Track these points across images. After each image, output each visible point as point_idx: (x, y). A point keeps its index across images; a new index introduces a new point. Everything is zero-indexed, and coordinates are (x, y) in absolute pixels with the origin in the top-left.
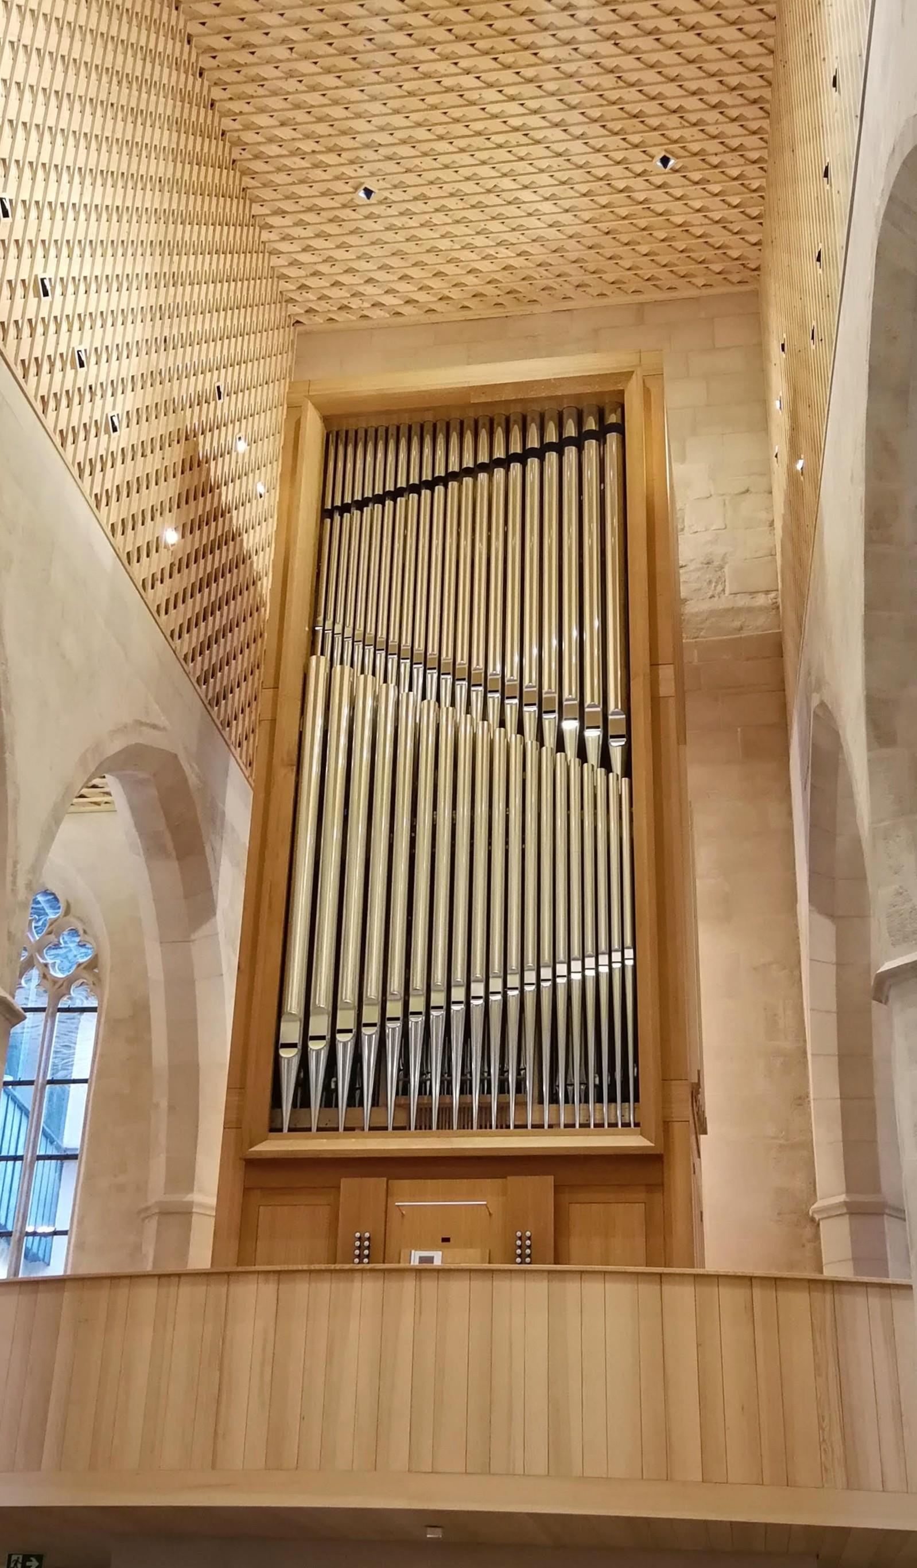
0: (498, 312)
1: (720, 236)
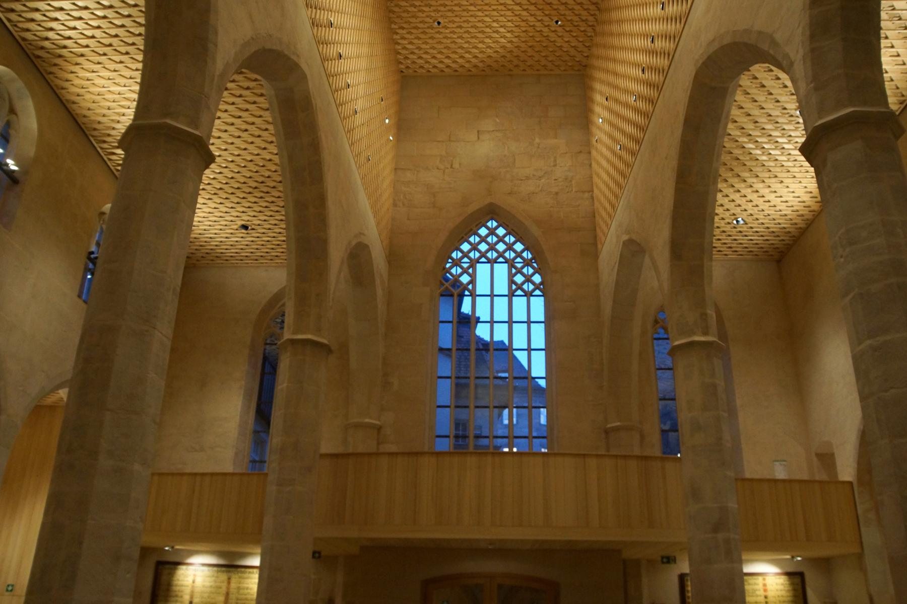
0: (483, 73)
1: (573, 52)
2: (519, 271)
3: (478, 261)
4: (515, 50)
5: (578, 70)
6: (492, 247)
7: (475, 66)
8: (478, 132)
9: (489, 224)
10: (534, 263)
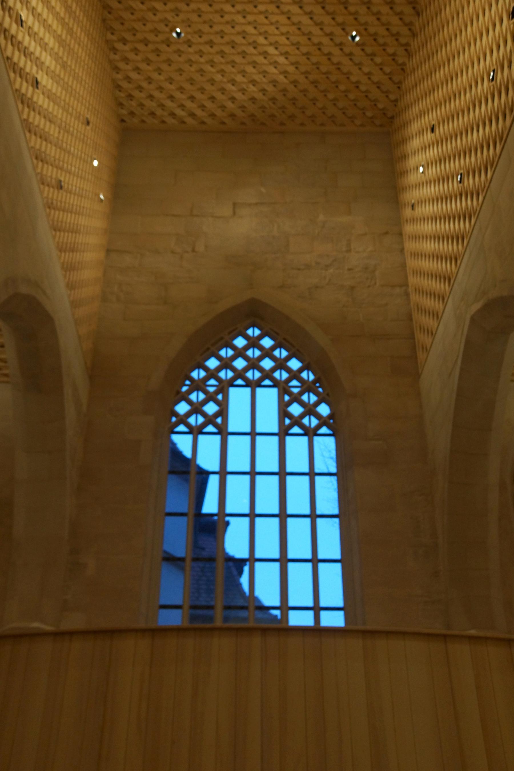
2: (296, 399)
3: (231, 383)
4: (291, 88)
5: (381, 126)
6: (253, 364)
7: (232, 116)
8: (234, 204)
9: (250, 332)
10: (318, 387)
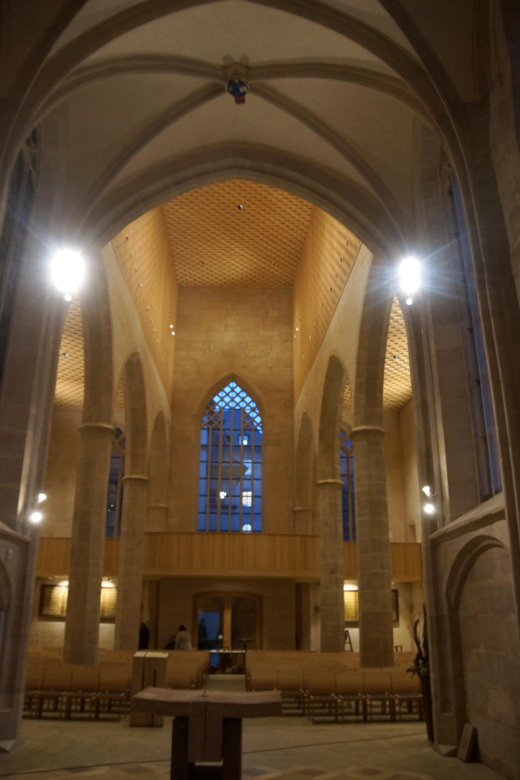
1: (284, 278)
8: (226, 326)
